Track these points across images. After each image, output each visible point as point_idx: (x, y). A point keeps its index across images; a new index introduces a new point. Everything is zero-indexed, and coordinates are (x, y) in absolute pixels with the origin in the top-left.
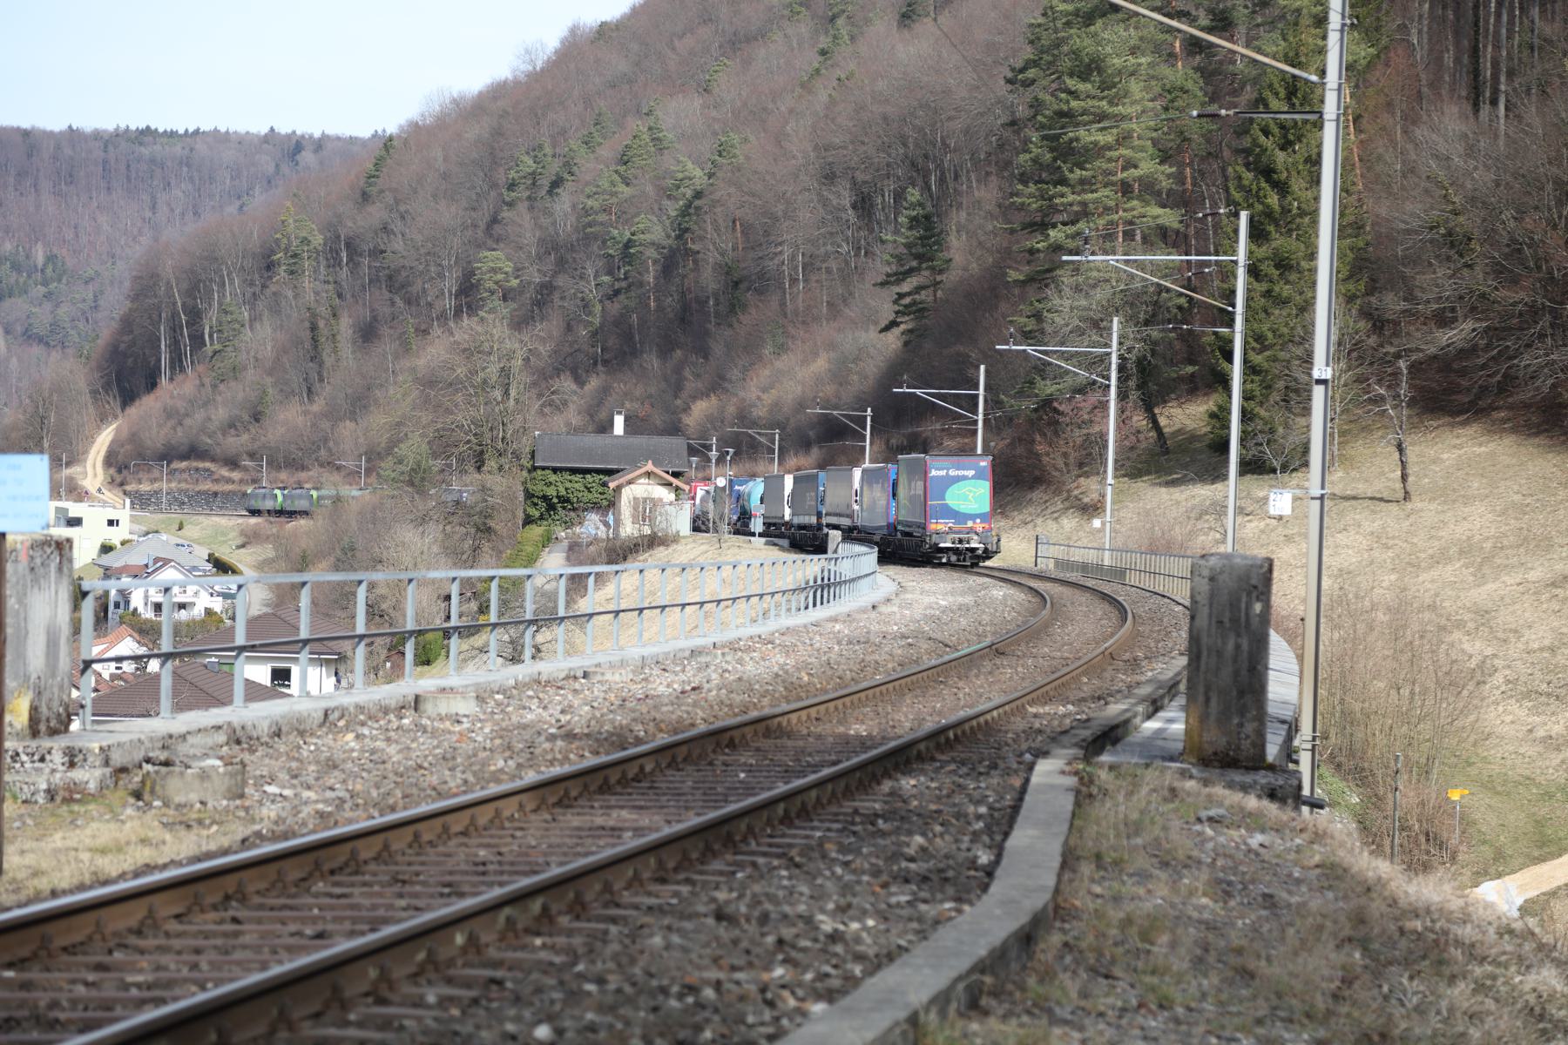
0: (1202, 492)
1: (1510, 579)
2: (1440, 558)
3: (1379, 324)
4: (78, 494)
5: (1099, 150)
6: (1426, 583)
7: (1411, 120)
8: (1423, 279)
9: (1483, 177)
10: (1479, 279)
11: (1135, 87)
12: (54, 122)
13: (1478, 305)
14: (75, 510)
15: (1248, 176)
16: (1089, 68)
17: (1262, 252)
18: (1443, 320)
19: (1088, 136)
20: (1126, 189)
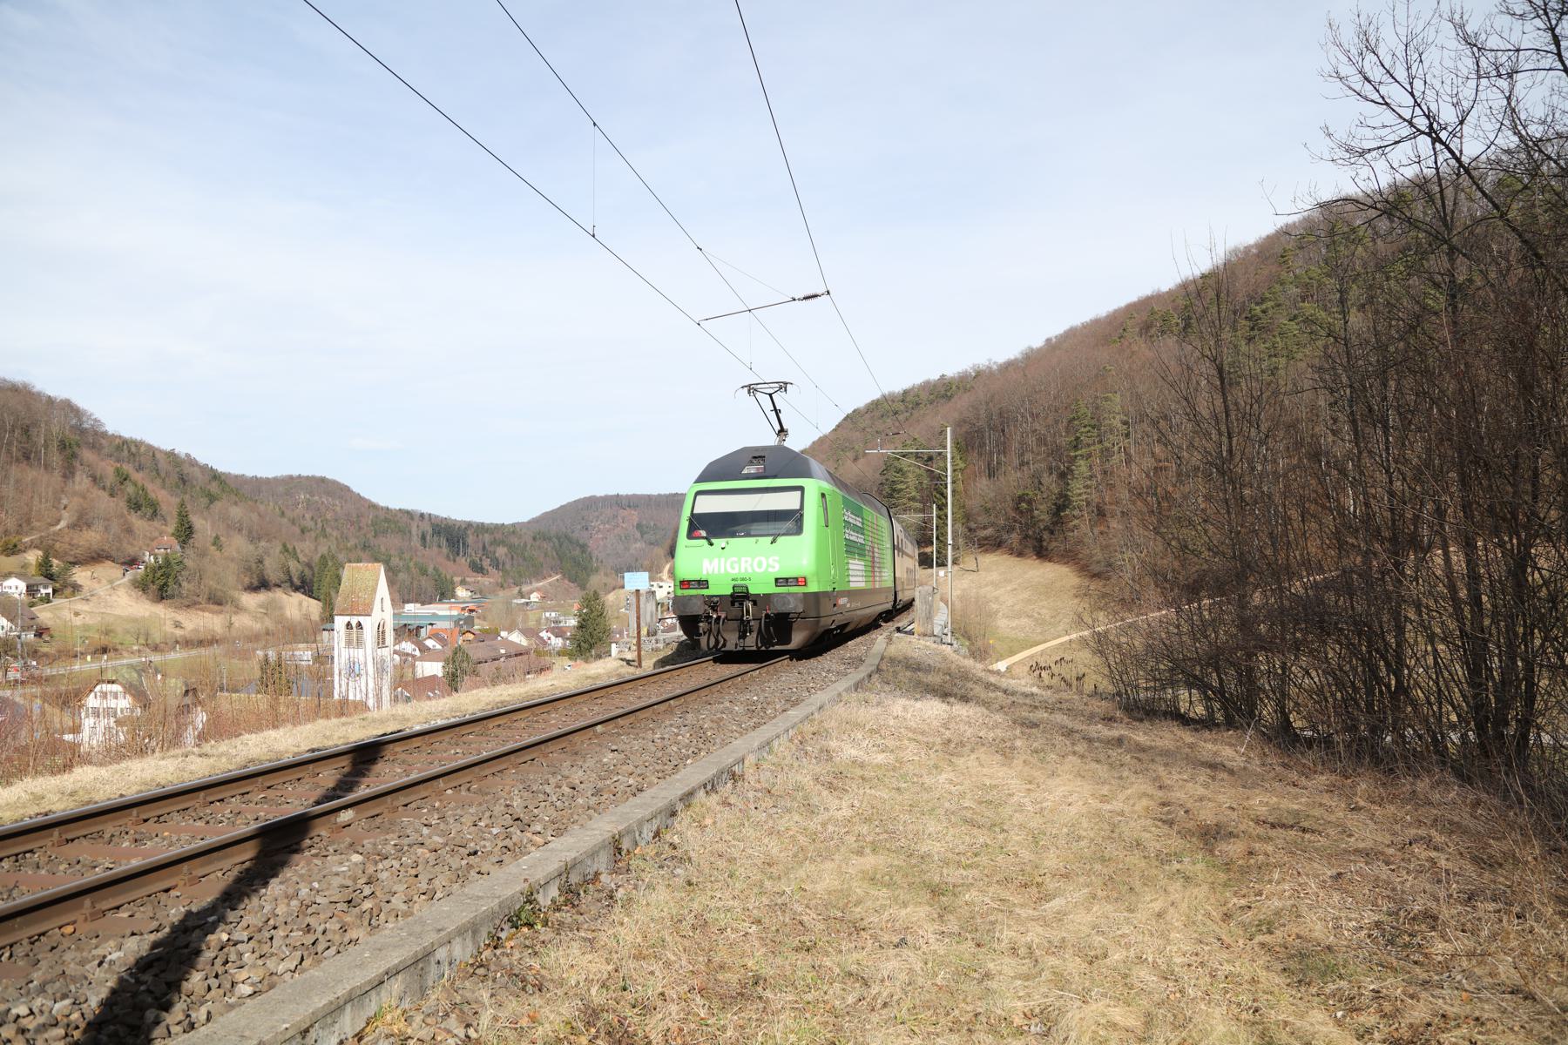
0: (929, 570)
1: (1003, 590)
2: (986, 585)
3: (970, 530)
4: (662, 580)
5: (900, 490)
6: (983, 591)
7: (975, 481)
8: (980, 518)
9: (992, 495)
10: (992, 518)
11: (910, 475)
12: (655, 492)
13: (993, 524)
14: (661, 584)
15: (938, 496)
16: (899, 471)
17: (941, 513)
18: (985, 528)
19: (899, 487)
20: (909, 499)
